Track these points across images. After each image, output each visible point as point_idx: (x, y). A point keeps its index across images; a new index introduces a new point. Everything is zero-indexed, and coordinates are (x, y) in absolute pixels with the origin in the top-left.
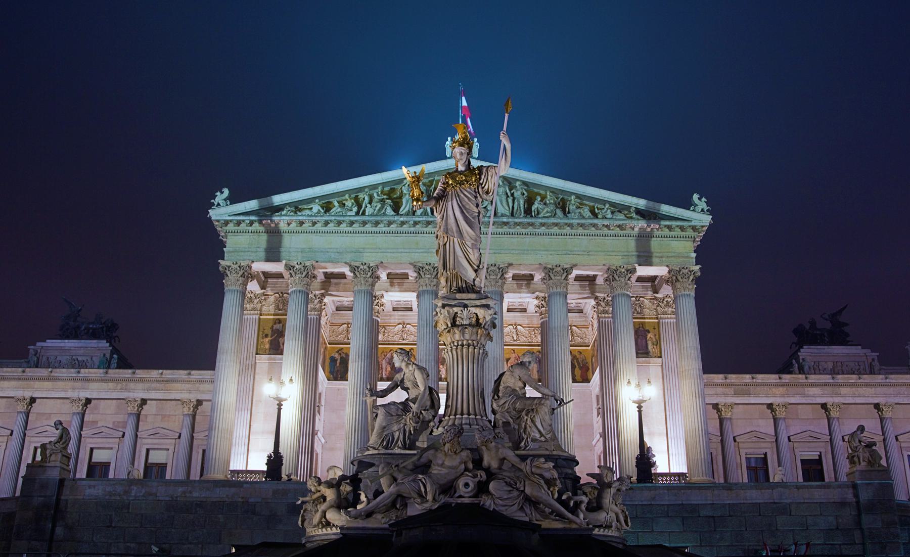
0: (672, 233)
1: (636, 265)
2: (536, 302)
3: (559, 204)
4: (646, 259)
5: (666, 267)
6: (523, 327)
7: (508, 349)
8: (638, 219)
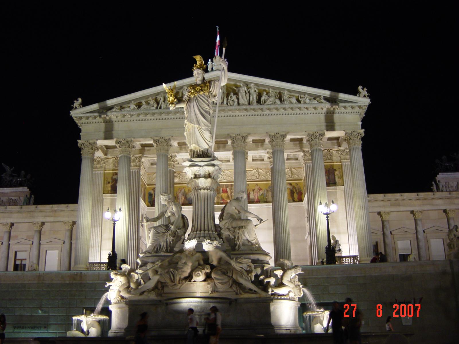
1: (325, 131)
2: (267, 155)
3: (277, 96)
4: (331, 126)
5: (343, 131)
6: (262, 170)
7: (254, 183)
8: (326, 103)
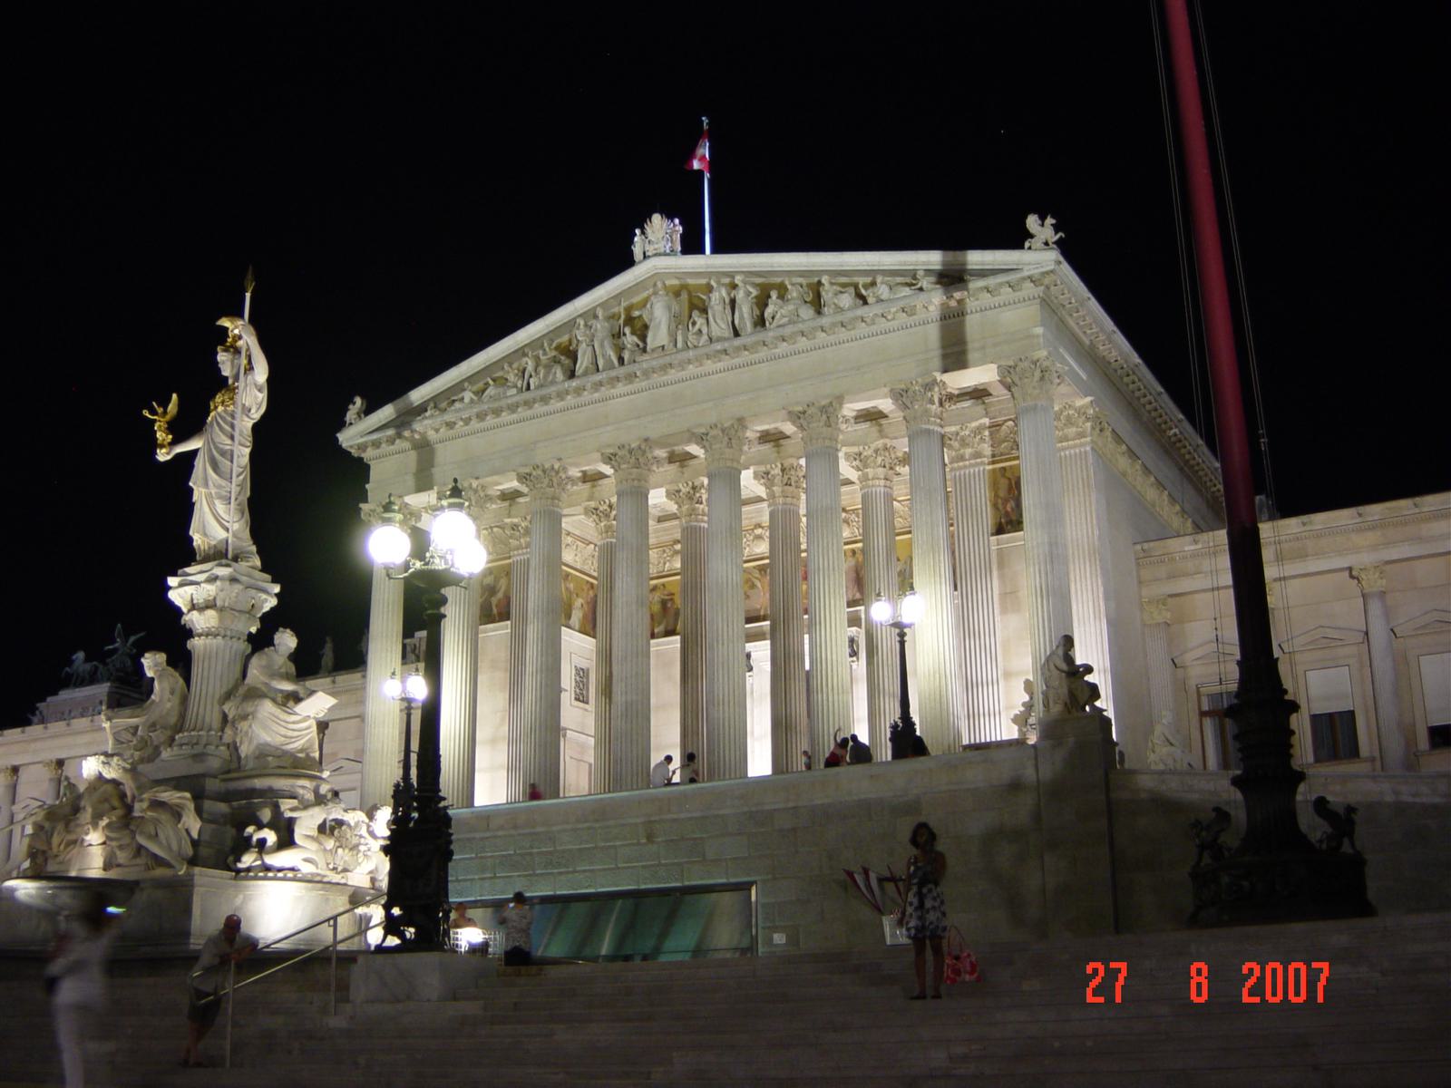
0: (997, 300)
4: (955, 356)
